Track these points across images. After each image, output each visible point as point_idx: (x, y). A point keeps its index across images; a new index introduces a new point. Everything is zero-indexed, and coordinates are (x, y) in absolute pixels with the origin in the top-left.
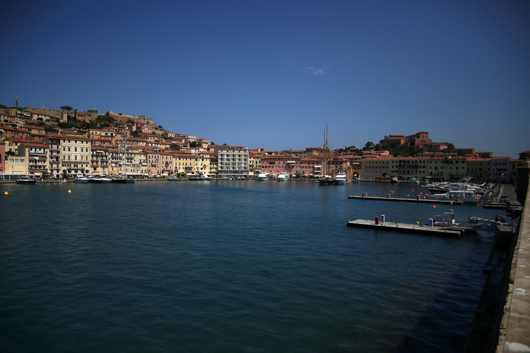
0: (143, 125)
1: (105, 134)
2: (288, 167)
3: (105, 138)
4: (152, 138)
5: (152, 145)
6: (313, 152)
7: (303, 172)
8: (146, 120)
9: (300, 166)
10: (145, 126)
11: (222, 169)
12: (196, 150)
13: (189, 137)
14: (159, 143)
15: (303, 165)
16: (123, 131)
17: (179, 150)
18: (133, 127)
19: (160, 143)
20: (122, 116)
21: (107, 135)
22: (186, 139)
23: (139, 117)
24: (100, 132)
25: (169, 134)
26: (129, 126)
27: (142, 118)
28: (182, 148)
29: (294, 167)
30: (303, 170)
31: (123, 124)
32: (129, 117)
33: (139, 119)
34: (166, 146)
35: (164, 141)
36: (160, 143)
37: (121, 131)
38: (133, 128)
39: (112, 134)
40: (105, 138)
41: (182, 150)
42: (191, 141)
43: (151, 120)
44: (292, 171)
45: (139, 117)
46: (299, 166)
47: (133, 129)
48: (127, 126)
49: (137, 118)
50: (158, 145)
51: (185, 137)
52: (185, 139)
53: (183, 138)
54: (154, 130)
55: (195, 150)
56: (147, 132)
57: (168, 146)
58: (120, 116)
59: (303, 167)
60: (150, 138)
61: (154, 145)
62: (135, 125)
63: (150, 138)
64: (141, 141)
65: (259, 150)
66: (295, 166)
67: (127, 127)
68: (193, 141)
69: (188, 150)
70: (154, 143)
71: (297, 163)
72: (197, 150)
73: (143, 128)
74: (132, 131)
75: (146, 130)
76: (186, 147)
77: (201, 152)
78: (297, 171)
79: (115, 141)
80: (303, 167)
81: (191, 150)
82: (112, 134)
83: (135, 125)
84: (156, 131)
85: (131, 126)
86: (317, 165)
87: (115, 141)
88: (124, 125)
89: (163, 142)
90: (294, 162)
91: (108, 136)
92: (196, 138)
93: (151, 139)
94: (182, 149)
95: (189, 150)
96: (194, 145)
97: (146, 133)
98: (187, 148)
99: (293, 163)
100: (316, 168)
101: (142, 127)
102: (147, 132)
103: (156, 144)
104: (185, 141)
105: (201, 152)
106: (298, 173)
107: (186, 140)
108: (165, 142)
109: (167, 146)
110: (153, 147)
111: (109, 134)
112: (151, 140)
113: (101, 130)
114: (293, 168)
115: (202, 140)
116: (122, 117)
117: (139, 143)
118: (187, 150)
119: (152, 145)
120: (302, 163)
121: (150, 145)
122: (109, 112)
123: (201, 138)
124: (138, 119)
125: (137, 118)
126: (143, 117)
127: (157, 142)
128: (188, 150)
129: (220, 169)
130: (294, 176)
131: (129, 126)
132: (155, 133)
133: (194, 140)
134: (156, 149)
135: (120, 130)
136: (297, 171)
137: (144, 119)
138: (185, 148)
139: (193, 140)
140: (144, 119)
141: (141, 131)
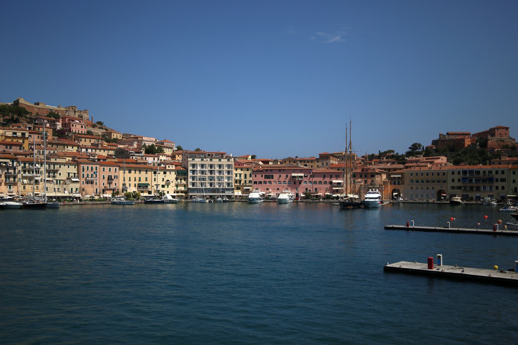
0: (73, 121)
1: (12, 133)
2: (292, 183)
3: (12, 140)
4: (88, 140)
5: (87, 150)
6: (330, 159)
7: (316, 189)
8: (77, 112)
9: (311, 180)
10: (76, 122)
11: (194, 186)
12: (154, 159)
13: (144, 138)
14: (98, 147)
15: (315, 179)
16: (41, 129)
17: (129, 158)
18: (57, 123)
19: (100, 148)
20: (39, 106)
21: (15, 135)
22: (140, 142)
23: (66, 108)
24: (4, 131)
25: (113, 134)
26: (51, 121)
27: (72, 110)
28: (134, 155)
29: (303, 183)
30: (315, 186)
31: (42, 119)
32: (51, 108)
33: (67, 111)
34: (109, 152)
35: (105, 144)
36: (100, 148)
37: (39, 129)
38: (56, 125)
39: (23, 134)
40: (12, 140)
41: (133, 158)
42: (147, 145)
43: (86, 113)
44: (299, 189)
45: (66, 108)
46: (310, 181)
47: (58, 126)
48: (48, 121)
49: (63, 109)
50: (96, 151)
51: (137, 138)
52: (138, 141)
53: (134, 141)
54: (90, 128)
55: (153, 158)
56: (79, 131)
57: (112, 153)
58: (36, 106)
59: (315, 182)
60: (83, 140)
61: (89, 151)
62: (61, 120)
63: (83, 140)
64: (70, 145)
65: (250, 157)
66: (304, 181)
67: (48, 123)
68: (150, 145)
69: (142, 158)
70: (89, 148)
71: (307, 177)
72: (156, 159)
73: (73, 125)
74: (56, 129)
75: (77, 128)
76: (139, 153)
77: (163, 160)
78: (307, 189)
79: (29, 144)
80: (315, 182)
81: (147, 158)
82: (23, 134)
83: (61, 120)
84: (93, 129)
85: (54, 122)
86: (337, 179)
87: (29, 144)
88: (43, 120)
89: (104, 145)
90: (302, 175)
91: (17, 137)
92: (154, 139)
93: (85, 141)
94: (134, 157)
95: (144, 157)
96: (151, 151)
97: (77, 132)
98: (140, 155)
99: (301, 177)
100: (335, 183)
101: (71, 124)
102: (79, 131)
103: (94, 149)
104: (138, 145)
105: (163, 160)
106: (308, 192)
107: (139, 143)
108: (106, 146)
109: (110, 151)
110: (88, 154)
111: (19, 134)
112: (85, 144)
113: (5, 128)
114: (300, 183)
115: (164, 142)
116: (40, 108)
117: (67, 148)
118: (141, 157)
119: (87, 150)
120: (313, 176)
121: (84, 150)
122: (18, 100)
123: (162, 140)
124: (65, 112)
125: (64, 109)
126: (72, 109)
127: (95, 146)
128: (142, 158)
129: (192, 186)
130: (302, 195)
131: (51, 121)
132: (92, 132)
133: (152, 143)
134: (92, 156)
135: (37, 129)
136: (307, 189)
137: (75, 112)
138: (138, 154)
139: (150, 144)
140: (75, 112)
141: (70, 129)
